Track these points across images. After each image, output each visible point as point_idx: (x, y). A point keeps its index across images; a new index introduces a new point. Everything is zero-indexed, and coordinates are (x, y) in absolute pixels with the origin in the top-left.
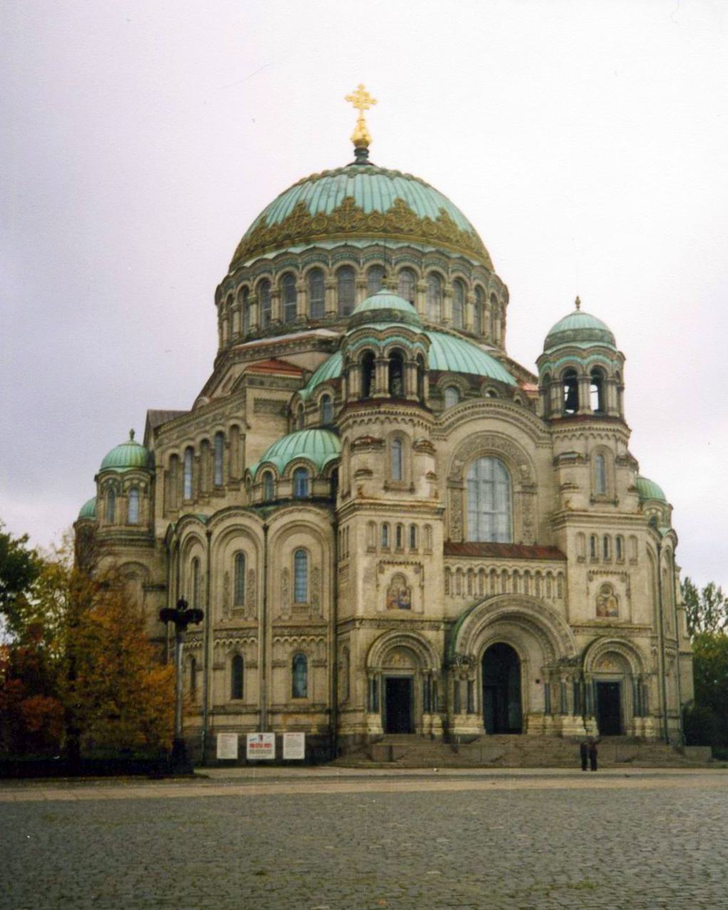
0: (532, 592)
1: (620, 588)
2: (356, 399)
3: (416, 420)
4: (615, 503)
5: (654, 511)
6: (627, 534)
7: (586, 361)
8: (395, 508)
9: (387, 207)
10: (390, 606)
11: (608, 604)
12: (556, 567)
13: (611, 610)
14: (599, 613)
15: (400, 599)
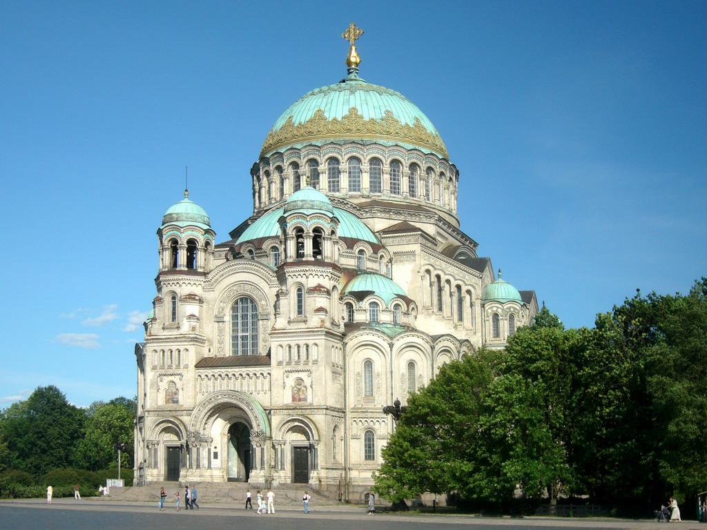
0: (245, 389)
1: (307, 382)
2: (167, 270)
3: (181, 282)
4: (305, 322)
5: (495, 309)
6: (310, 343)
7: (309, 224)
8: (167, 340)
9: (308, 118)
10: (167, 402)
11: (301, 393)
12: (265, 370)
13: (302, 397)
14: (294, 399)
15: (172, 398)
